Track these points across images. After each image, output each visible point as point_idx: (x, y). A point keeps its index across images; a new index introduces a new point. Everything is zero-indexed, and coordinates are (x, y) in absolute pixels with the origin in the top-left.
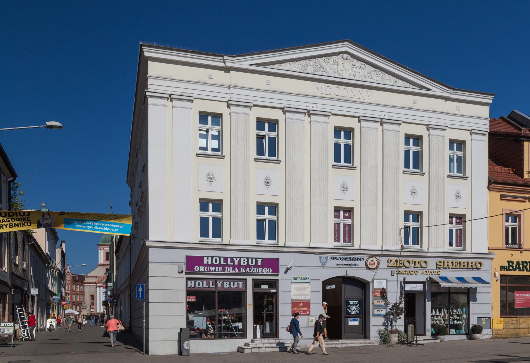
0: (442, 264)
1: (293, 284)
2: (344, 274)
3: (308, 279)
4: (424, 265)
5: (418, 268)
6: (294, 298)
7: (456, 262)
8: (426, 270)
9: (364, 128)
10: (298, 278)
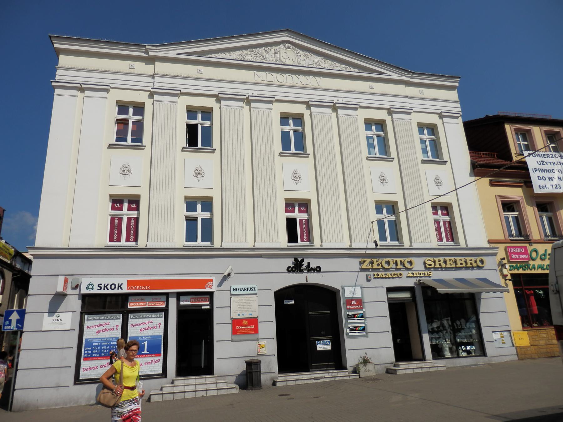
0: (433, 263)
1: (233, 297)
3: (254, 289)
4: (408, 266)
5: (402, 270)
6: (235, 316)
8: (412, 272)
9: (315, 114)
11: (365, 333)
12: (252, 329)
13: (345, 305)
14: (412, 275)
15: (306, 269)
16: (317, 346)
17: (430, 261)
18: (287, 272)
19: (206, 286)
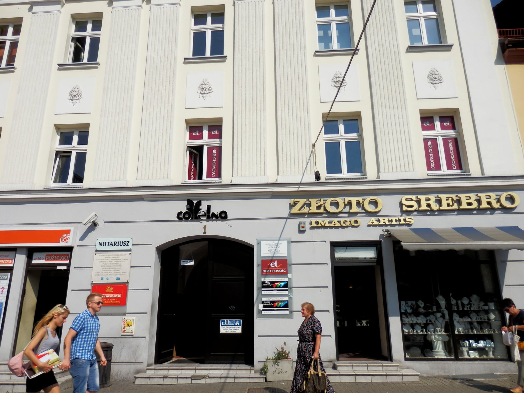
3: (126, 243)
5: (359, 215)
6: (97, 280)
8: (377, 218)
10: (108, 242)
11: (288, 311)
12: (118, 299)
13: (260, 267)
14: (376, 223)
15: (205, 215)
16: (221, 327)
17: (412, 200)
18: (177, 219)
19: (60, 239)
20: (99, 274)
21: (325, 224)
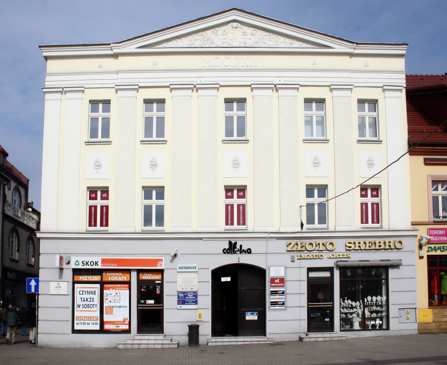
1: (179, 274)
2: (236, 262)
3: (195, 268)
5: (324, 251)
7: (369, 243)
8: (332, 254)
13: (270, 282)
14: (332, 257)
15: (238, 251)
19: (157, 265)
20: (181, 286)
21: (305, 257)
